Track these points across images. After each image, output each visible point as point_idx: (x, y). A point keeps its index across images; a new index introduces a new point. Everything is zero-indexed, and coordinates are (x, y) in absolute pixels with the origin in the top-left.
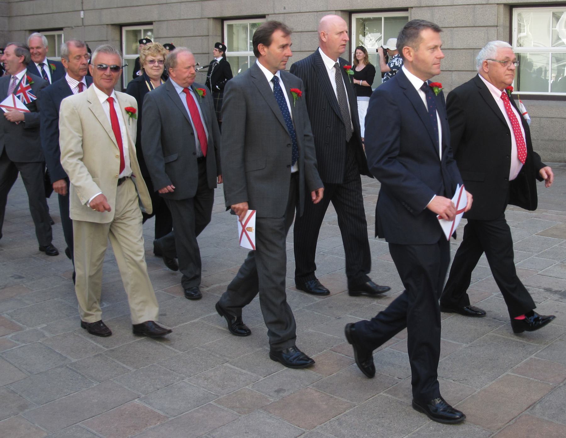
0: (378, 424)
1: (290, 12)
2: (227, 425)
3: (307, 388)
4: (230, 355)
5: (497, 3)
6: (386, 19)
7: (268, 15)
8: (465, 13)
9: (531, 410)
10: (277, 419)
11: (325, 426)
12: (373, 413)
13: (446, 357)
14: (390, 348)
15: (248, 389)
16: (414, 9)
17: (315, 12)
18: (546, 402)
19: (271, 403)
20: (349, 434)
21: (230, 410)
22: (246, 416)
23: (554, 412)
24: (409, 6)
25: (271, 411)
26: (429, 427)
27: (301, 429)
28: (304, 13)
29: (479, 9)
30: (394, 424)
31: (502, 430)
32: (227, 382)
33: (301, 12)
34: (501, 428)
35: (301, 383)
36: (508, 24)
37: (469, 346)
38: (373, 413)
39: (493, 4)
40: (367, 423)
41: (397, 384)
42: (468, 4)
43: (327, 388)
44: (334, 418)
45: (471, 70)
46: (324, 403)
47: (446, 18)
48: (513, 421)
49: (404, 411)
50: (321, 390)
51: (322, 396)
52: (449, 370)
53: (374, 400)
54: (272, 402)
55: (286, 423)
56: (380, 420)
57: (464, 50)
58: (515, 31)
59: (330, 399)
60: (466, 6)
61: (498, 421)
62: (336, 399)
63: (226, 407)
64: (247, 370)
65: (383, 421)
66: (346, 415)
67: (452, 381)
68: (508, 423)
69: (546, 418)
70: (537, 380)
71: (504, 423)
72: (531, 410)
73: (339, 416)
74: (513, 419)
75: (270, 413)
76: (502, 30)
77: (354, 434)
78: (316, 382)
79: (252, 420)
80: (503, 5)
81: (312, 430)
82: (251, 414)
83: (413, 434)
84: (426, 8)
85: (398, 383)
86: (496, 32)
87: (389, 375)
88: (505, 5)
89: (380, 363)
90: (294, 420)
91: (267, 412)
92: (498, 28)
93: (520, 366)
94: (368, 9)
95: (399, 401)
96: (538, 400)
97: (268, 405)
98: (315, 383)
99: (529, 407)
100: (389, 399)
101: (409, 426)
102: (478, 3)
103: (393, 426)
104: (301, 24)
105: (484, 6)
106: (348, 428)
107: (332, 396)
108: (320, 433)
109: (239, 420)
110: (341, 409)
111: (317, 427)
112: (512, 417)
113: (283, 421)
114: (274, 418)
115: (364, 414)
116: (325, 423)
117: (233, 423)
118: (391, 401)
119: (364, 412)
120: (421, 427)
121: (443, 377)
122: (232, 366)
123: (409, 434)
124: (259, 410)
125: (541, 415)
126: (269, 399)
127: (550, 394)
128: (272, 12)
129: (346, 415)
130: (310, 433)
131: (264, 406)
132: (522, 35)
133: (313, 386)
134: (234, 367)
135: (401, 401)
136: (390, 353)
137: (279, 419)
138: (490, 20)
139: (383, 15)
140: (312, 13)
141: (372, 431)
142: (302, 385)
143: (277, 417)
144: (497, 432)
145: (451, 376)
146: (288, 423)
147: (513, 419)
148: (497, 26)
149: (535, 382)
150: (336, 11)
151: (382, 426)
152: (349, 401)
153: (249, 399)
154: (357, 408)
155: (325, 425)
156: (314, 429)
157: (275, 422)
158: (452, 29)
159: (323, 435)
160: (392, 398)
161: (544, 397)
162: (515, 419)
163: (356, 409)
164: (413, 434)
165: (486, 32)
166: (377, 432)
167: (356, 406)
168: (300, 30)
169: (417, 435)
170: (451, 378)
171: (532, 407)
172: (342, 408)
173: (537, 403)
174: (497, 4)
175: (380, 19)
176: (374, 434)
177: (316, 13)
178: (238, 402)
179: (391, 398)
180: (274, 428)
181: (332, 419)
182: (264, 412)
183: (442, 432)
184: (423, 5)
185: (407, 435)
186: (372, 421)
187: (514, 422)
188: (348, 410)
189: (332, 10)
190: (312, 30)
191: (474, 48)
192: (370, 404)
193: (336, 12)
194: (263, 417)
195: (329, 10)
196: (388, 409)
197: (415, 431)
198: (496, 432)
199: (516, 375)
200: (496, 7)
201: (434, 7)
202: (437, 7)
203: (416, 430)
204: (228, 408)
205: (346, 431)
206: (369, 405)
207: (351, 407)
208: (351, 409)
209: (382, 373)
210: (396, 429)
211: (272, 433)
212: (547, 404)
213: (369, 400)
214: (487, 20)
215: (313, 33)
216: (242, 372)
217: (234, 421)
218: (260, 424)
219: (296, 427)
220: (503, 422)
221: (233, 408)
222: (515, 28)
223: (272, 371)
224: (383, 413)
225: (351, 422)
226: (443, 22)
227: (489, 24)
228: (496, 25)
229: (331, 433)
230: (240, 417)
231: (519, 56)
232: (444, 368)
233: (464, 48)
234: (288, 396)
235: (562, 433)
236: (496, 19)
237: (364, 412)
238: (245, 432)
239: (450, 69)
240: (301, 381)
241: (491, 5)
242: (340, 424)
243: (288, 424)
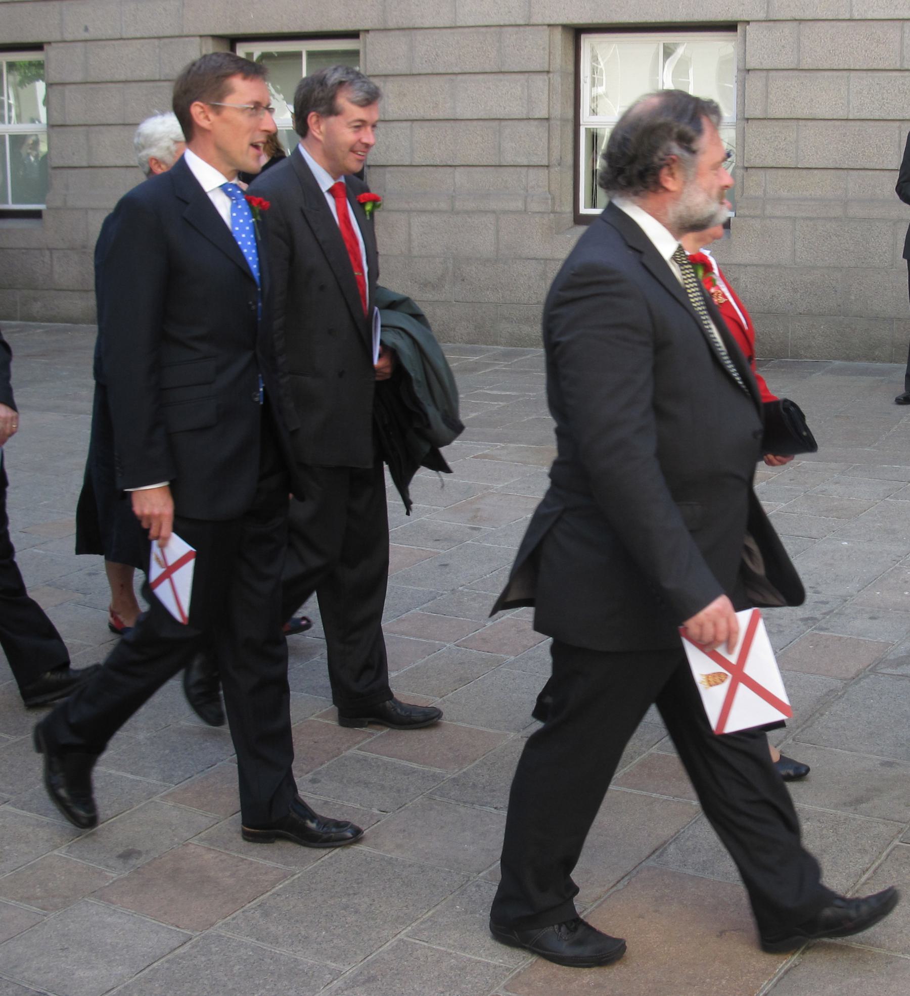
0: (345, 908)
1: (100, 37)
2: (18, 936)
3: (187, 845)
4: (10, 787)
5: (547, 22)
6: (311, 55)
7: (49, 43)
8: (481, 43)
9: (659, 857)
10: (129, 915)
11: (234, 922)
12: (334, 886)
13: (477, 762)
14: (358, 749)
15: (58, 856)
16: (371, 34)
17: (155, 38)
18: (688, 839)
19: (111, 881)
20: (286, 934)
21: (21, 904)
22: (59, 915)
23: (705, 858)
24: (361, 28)
25: (114, 899)
26: (454, 906)
27: (182, 931)
28: (130, 42)
29: (510, 35)
30: (380, 906)
31: (604, 901)
32: (9, 844)
33: (124, 36)
34: (600, 898)
35: (174, 835)
36: (571, 68)
37: (522, 737)
38: (334, 886)
39: (538, 25)
40: (322, 908)
41: (379, 823)
42: (486, 24)
43: (231, 842)
44: (252, 903)
45: (493, 164)
46: (228, 874)
47: (441, 54)
48: (625, 882)
49: (398, 878)
50: (218, 846)
51: (221, 860)
52: (484, 788)
53: (333, 859)
54: (114, 879)
55: (148, 922)
56: (349, 900)
57: (481, 123)
58: (586, 82)
59: (241, 863)
60: (484, 30)
61: (593, 884)
62: (251, 863)
63: (13, 899)
64: (51, 816)
65: (356, 901)
66: (278, 895)
67: (493, 809)
68: (614, 885)
69: (691, 872)
70: (665, 797)
71: (606, 888)
72: (659, 857)
73: (261, 898)
74: (623, 878)
75: (113, 903)
76: (559, 79)
77: (297, 933)
78: (206, 831)
79: (73, 922)
80: (560, 29)
81: (207, 931)
82: (71, 909)
83: (422, 923)
84: (397, 33)
85: (381, 821)
86: (547, 83)
87: (361, 804)
88: (565, 27)
89: (339, 783)
90: (165, 914)
91: (107, 903)
92: (551, 75)
93: (628, 770)
94: (271, 34)
95: (386, 859)
96: (672, 837)
97: (108, 886)
98: (204, 833)
99: (654, 852)
100: (364, 855)
101: (411, 908)
102: (507, 23)
103: (378, 910)
104: (124, 65)
105: (522, 29)
106: (285, 921)
107: (244, 857)
108: (224, 937)
109: (46, 924)
110: (266, 883)
111: (218, 924)
112: (622, 875)
113: (143, 918)
114: (122, 913)
115: (315, 890)
116: (234, 915)
117: (32, 931)
118: (369, 859)
119: (313, 886)
120: (438, 907)
121: (473, 804)
122: (18, 810)
123: (413, 925)
124: (86, 899)
125: (679, 866)
126: (107, 874)
127: (694, 823)
128: (59, 38)
129: (278, 895)
130: (203, 938)
131: (97, 889)
132: (600, 90)
133: (201, 840)
134: (22, 811)
135: (392, 858)
136: (358, 761)
137: (132, 915)
138: (535, 58)
139: (304, 47)
140: (147, 41)
141: (336, 924)
142: (176, 839)
143: (129, 910)
144: (594, 906)
145: (489, 799)
146: (153, 921)
147: (623, 878)
148: (548, 72)
149: (661, 801)
150: (201, 36)
151: (356, 912)
152: (280, 865)
153: (63, 878)
154: (299, 878)
155: (234, 919)
156: (211, 930)
157: (126, 922)
158: (453, 77)
159: (231, 940)
160: (370, 852)
161: (682, 830)
162: (627, 878)
163: (296, 881)
164: (422, 923)
165: (526, 84)
166: (347, 926)
167: (296, 874)
168: (122, 77)
169: (430, 923)
170: (490, 803)
171: (661, 850)
172: (267, 881)
173: (670, 844)
174: (549, 25)
175: (298, 55)
176: (341, 930)
177: (156, 42)
178: (38, 886)
179: (368, 853)
180: (124, 934)
181: (249, 905)
182: (99, 902)
183: (481, 914)
184: (391, 25)
185: (409, 925)
186: (331, 902)
187: (626, 883)
188: (280, 885)
189: (191, 33)
190: (149, 78)
191: (501, 118)
192: (326, 869)
193: (203, 39)
194: (97, 914)
195: (185, 33)
196: (365, 876)
197: (424, 917)
198: (592, 905)
199: (623, 789)
200: (546, 31)
201: (415, 31)
202: (422, 31)
203: (427, 915)
204: (17, 901)
205: (280, 928)
206: (323, 870)
207: (285, 877)
208: (287, 882)
209: (346, 803)
210: (384, 915)
211: (120, 946)
212: (689, 843)
213: (322, 859)
214: (528, 59)
215: (151, 84)
216: (42, 822)
217: (33, 928)
218: (92, 929)
219: (173, 928)
220: (605, 885)
221: (28, 899)
222: (587, 77)
223: (107, 815)
224: (355, 885)
225: (289, 908)
226: (434, 62)
227: (532, 68)
228: (546, 69)
229: (248, 934)
230: (45, 918)
231: (593, 136)
232: (474, 784)
233: (479, 117)
234: (149, 864)
235: (725, 898)
236: (547, 57)
237: (313, 886)
238: (61, 949)
239: (449, 163)
240: (173, 831)
241: (536, 28)
242: (266, 914)
243: (155, 924)
